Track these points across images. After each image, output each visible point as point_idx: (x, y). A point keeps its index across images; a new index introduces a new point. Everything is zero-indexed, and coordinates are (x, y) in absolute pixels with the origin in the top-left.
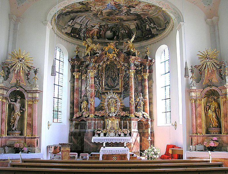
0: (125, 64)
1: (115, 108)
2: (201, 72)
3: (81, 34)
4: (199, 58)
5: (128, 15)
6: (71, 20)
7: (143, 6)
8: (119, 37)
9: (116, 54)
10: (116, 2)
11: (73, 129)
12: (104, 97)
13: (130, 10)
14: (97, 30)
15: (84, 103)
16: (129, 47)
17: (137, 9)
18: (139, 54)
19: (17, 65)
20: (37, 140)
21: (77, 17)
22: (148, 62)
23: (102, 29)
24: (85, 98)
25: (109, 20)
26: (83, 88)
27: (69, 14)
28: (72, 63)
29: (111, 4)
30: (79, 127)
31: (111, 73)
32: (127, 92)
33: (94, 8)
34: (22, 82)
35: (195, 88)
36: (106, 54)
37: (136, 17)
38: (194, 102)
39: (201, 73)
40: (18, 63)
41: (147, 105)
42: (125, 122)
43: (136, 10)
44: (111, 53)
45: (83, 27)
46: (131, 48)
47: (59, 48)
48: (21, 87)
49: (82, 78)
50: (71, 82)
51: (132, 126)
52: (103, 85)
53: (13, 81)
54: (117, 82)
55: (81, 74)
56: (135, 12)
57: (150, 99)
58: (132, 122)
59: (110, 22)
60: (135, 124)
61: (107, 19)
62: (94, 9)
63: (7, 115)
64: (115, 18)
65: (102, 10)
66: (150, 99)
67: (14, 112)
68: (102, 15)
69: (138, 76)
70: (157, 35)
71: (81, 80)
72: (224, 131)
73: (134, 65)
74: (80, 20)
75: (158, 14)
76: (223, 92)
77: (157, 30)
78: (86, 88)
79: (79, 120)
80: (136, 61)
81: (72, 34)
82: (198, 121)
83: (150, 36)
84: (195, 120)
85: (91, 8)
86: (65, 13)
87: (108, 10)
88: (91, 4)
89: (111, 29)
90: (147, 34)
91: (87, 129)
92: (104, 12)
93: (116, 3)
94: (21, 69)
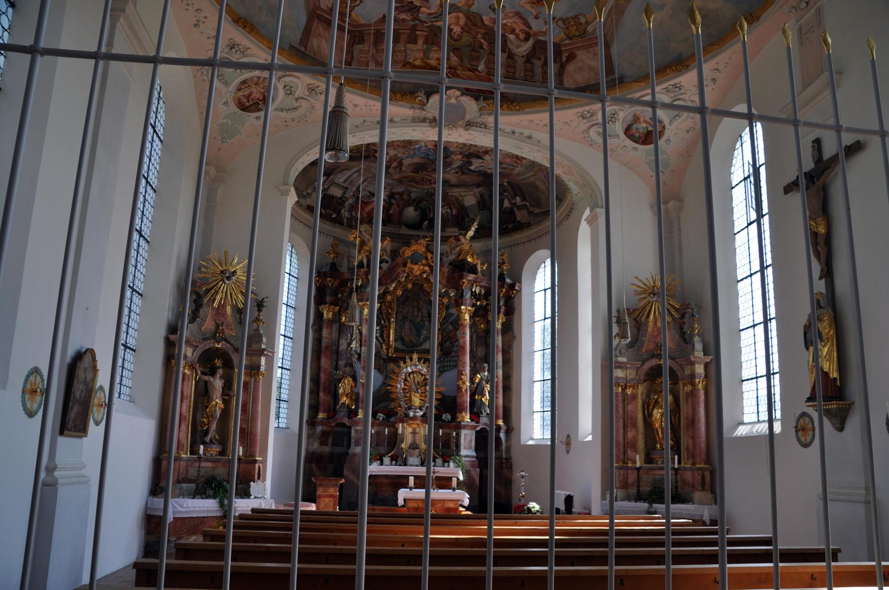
0: (450, 291)
1: (423, 398)
2: (639, 326)
3: (343, 211)
4: (636, 293)
5: (463, 173)
11: (316, 446)
12: (396, 370)
13: (471, 164)
15: (346, 382)
16: (461, 250)
17: (485, 162)
18: (485, 268)
19: (219, 288)
20: (259, 467)
21: (339, 170)
22: (504, 290)
23: (393, 201)
24: (348, 369)
25: (416, 183)
26: (343, 346)
29: (426, 146)
30: (330, 441)
31: (411, 310)
32: (449, 359)
34: (227, 329)
35: (624, 360)
36: (405, 265)
37: (481, 179)
38: (620, 391)
39: (638, 326)
40: (221, 282)
41: (497, 392)
42: (447, 431)
43: (485, 163)
44: (416, 264)
45: (349, 194)
46: (467, 253)
48: (226, 340)
49: (340, 319)
50: (314, 327)
51: (462, 441)
52: (391, 339)
53: (209, 325)
54: (424, 332)
55: (339, 310)
56: (481, 168)
57: (507, 378)
58: (464, 432)
59: (415, 187)
60: (468, 439)
63: (192, 404)
64: (429, 178)
65: (404, 156)
66: (507, 378)
67: (208, 398)
68: (401, 169)
69: (478, 321)
70: (529, 225)
71: (338, 324)
72: (686, 457)
73: (472, 295)
74: (345, 177)
75: (534, 175)
76: (688, 372)
77: (530, 213)
78: (349, 344)
79: (333, 424)
80: (476, 286)
82: (630, 435)
83: (510, 226)
84: (621, 432)
87: (416, 160)
89: (417, 203)
91: (352, 446)
92: (406, 162)
94: (229, 298)
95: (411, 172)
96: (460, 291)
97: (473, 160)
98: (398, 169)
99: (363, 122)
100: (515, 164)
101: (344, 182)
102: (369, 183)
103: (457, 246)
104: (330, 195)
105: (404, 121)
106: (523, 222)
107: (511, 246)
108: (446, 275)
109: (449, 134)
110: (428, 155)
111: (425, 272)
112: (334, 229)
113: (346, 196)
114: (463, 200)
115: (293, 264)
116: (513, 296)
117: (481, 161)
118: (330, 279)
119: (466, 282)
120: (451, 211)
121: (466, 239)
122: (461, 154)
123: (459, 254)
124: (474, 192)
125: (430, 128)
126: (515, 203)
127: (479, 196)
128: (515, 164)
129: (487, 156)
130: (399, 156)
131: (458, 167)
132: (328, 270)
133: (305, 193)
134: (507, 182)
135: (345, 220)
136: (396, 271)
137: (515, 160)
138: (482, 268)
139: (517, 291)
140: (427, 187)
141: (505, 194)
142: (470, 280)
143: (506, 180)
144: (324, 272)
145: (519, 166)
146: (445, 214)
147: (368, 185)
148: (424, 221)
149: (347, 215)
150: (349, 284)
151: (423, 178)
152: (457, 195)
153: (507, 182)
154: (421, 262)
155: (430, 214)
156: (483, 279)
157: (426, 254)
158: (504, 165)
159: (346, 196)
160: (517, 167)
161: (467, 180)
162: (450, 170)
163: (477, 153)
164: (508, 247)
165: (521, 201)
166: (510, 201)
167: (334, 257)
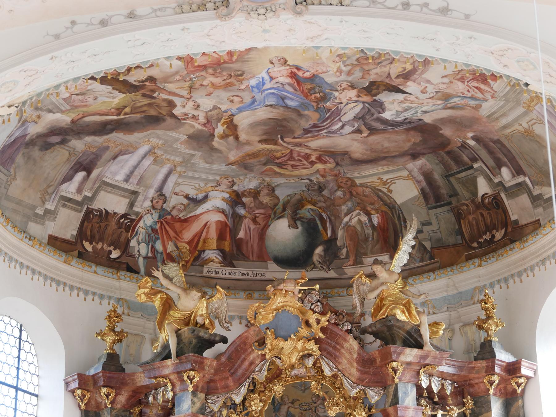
3: (133, 243)
5: (373, 131)
6: (76, 171)
7: (446, 80)
8: (340, 249)
9: (318, 341)
10: (298, 68)
13: (381, 106)
14: (221, 217)
17: (412, 98)
18: (441, 332)
21: (107, 155)
22: (495, 378)
23: (241, 211)
25: (281, 165)
27: (63, 142)
28: (82, 397)
29: (272, 78)
33: (190, 104)
36: (262, 343)
43: (411, 102)
46: (396, 303)
47: (14, 323)
56: (408, 114)
59: (281, 175)
61: (263, 159)
62: (189, 109)
64: (304, 151)
65: (234, 110)
68: (237, 138)
74: (126, 170)
75: (525, 114)
80: (431, 375)
81: (87, 245)
83: (499, 235)
85: (172, 104)
86: (40, 136)
87: (262, 114)
88: (170, 87)
90: (482, 227)
93: (300, 74)
95: (260, 142)
96: (391, 390)
97: (385, 97)
98: (231, 138)
99: (69, 25)
100: (479, 95)
101: (126, 180)
102: (180, 176)
103: (372, 290)
104: (101, 211)
105: (158, 13)
106: (523, 222)
107: (506, 280)
108: (355, 356)
109: (265, 31)
110: (283, 98)
111: (309, 355)
112: (116, 283)
113: (136, 209)
114: (391, 191)
115: (24, 366)
116: (519, 391)
117: (400, 96)
118: (104, 390)
119: (401, 369)
120: (370, 220)
121: (391, 272)
122: (352, 87)
123: (379, 307)
124: (410, 172)
125: (218, 22)
126: (501, 184)
127: (421, 178)
128: (479, 95)
129: (409, 83)
130: (224, 108)
131: (356, 118)
132: (100, 369)
133: (40, 211)
134: (473, 138)
135: (141, 260)
136: (245, 359)
137: (476, 85)
138: (433, 333)
139: (528, 378)
140: (305, 172)
141: (476, 166)
142: (409, 364)
143: (470, 135)
144: (93, 376)
145: (488, 96)
146: (359, 228)
147: (180, 180)
148: (315, 247)
149: (143, 252)
150: (151, 398)
151: (292, 151)
152: (374, 179)
153: (473, 138)
154: (296, 332)
155: (326, 230)
156: (441, 358)
157: (303, 313)
158: (455, 101)
159: (136, 209)
160: (485, 100)
161: (386, 144)
162: (342, 127)
163: (387, 81)
164: (499, 281)
165: (514, 176)
166: (489, 180)
167: (114, 342)
